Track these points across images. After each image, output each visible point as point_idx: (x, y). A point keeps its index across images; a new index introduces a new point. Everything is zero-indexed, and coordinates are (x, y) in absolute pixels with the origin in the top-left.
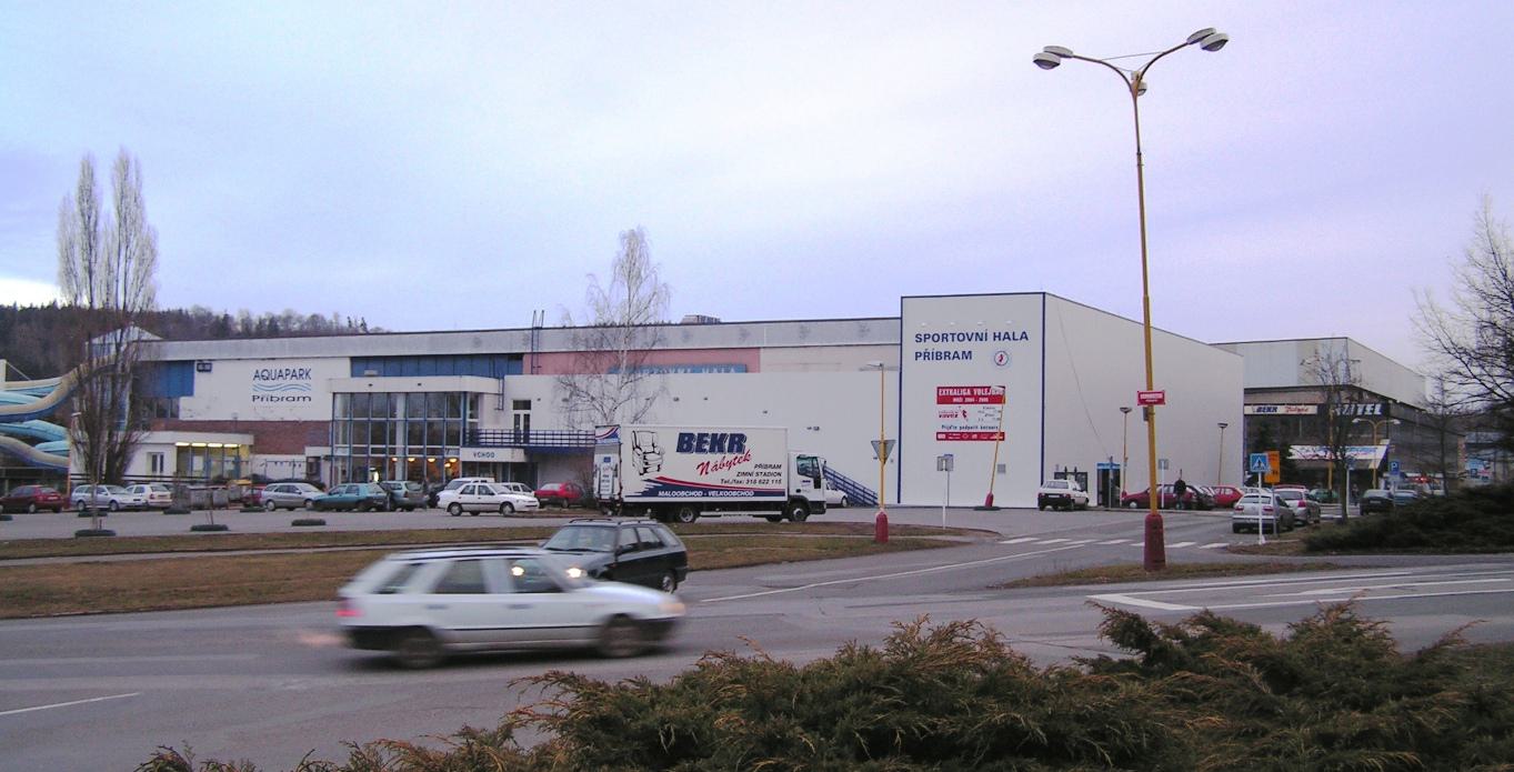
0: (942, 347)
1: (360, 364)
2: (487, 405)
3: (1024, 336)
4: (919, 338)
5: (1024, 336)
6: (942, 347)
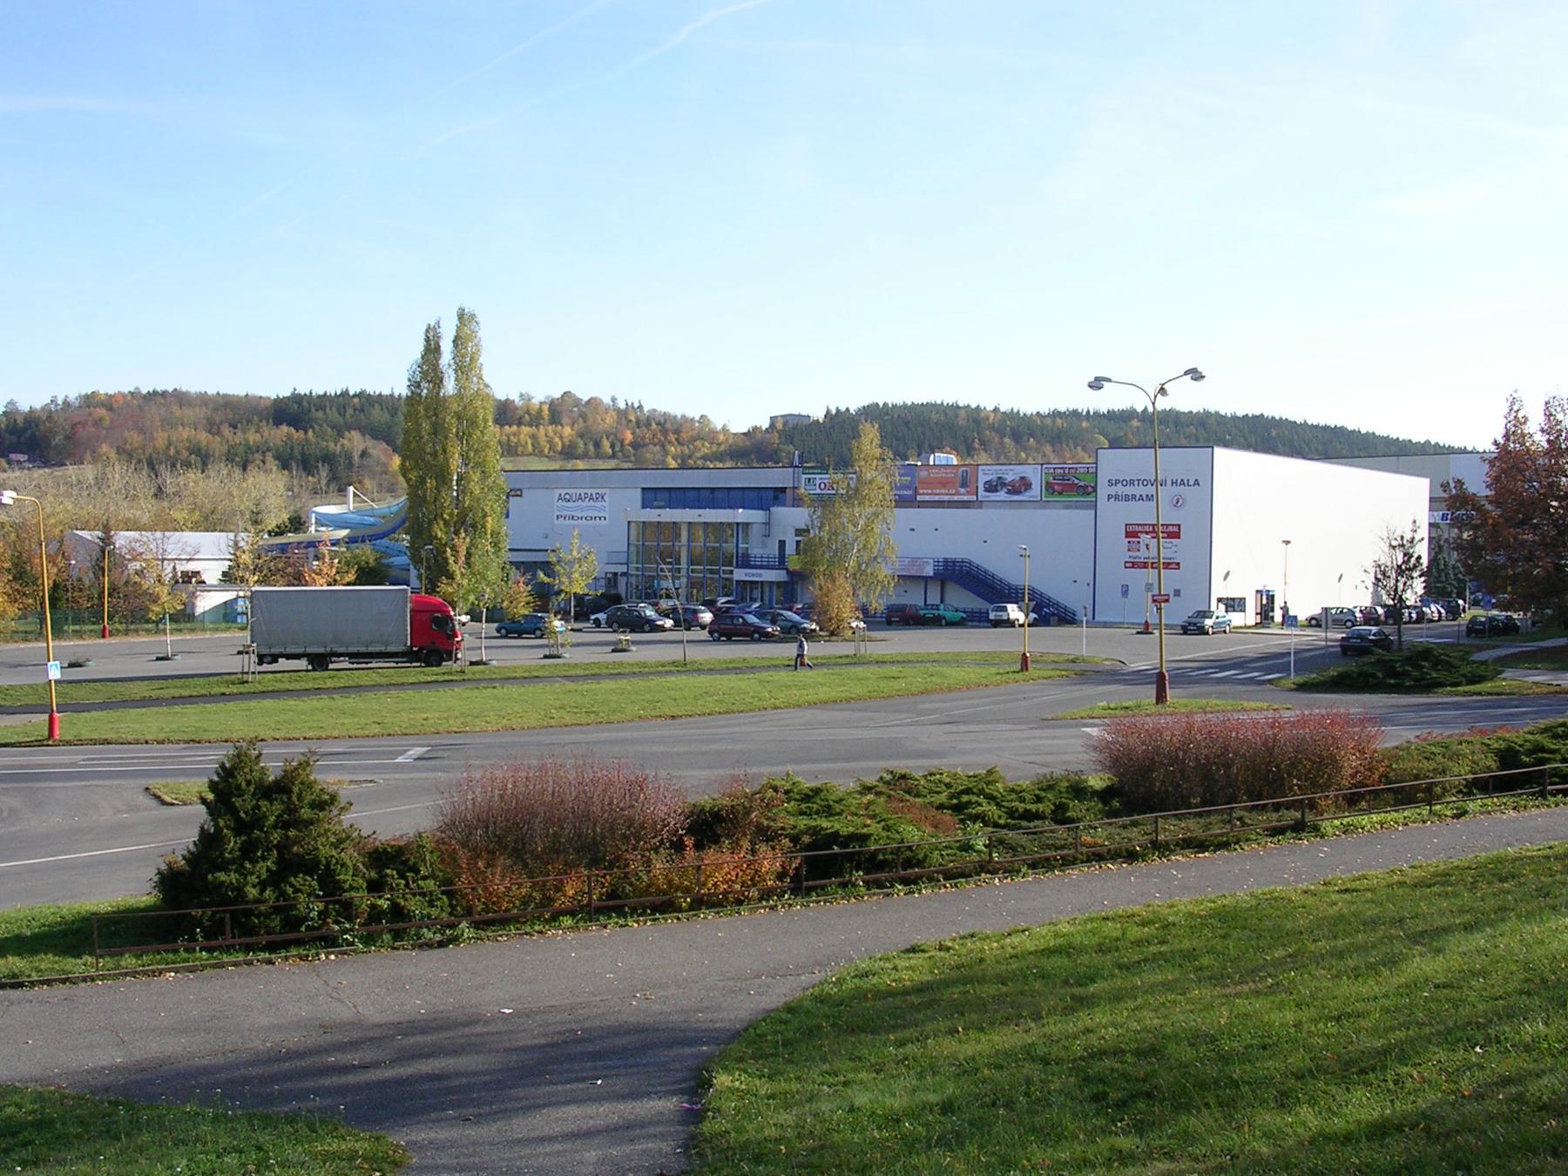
0: (1129, 490)
1: (652, 497)
2: (755, 532)
3: (1197, 483)
4: (1110, 483)
5: (1197, 483)
6: (1129, 490)
